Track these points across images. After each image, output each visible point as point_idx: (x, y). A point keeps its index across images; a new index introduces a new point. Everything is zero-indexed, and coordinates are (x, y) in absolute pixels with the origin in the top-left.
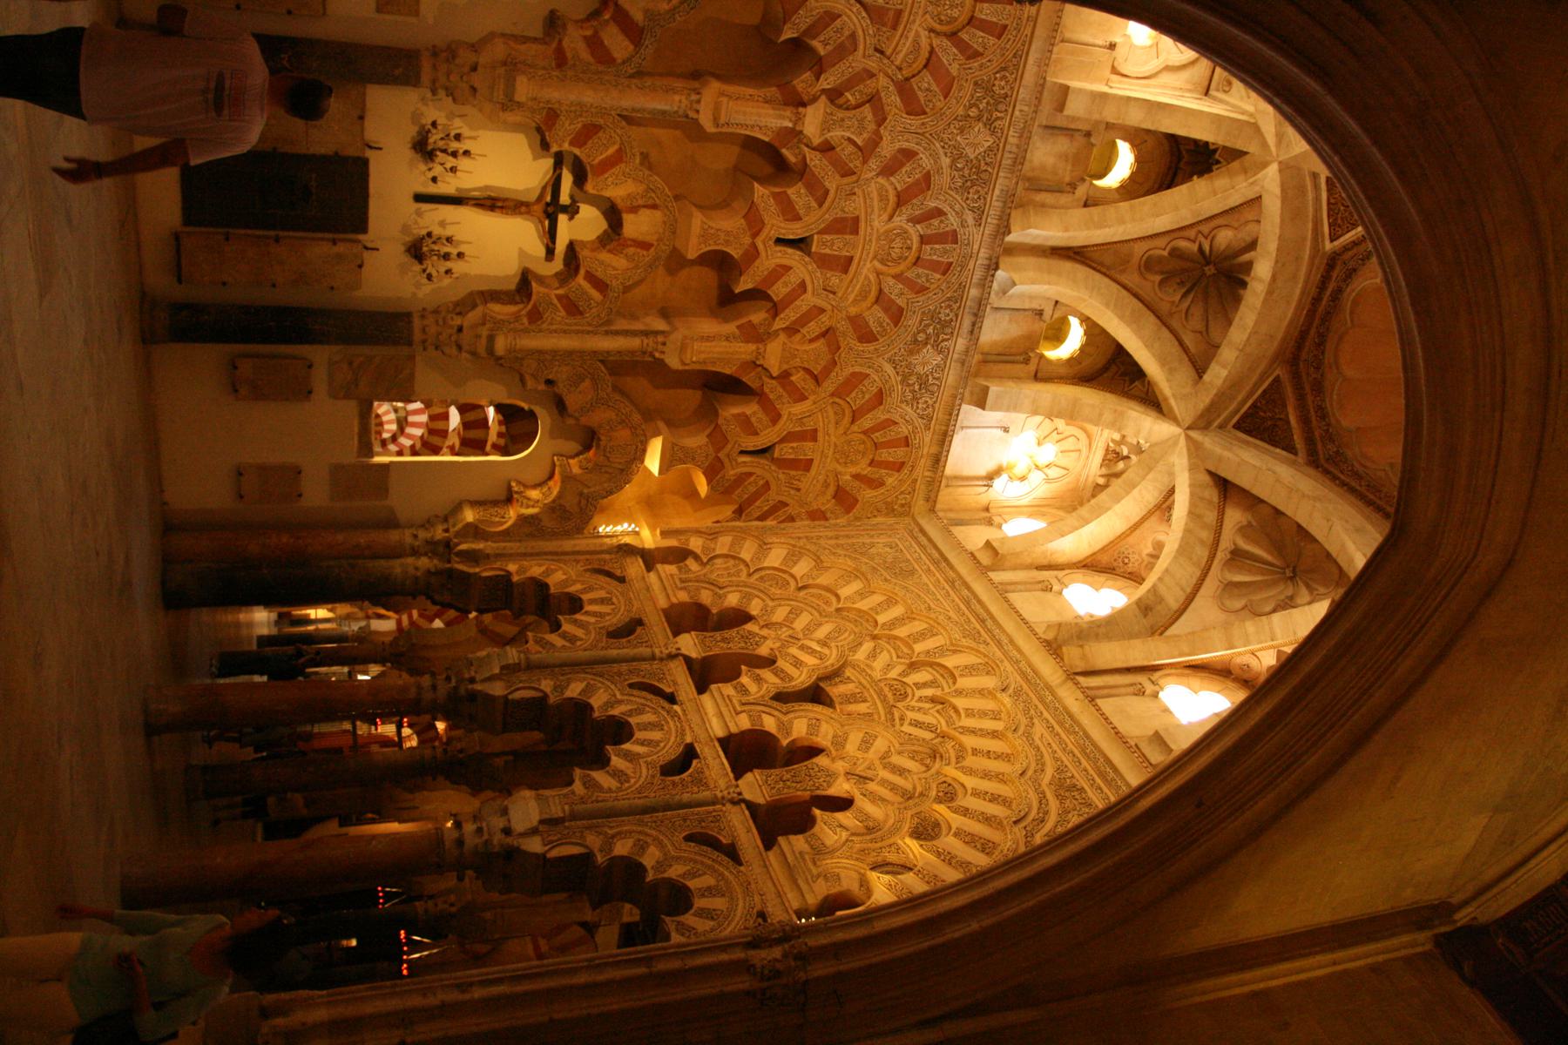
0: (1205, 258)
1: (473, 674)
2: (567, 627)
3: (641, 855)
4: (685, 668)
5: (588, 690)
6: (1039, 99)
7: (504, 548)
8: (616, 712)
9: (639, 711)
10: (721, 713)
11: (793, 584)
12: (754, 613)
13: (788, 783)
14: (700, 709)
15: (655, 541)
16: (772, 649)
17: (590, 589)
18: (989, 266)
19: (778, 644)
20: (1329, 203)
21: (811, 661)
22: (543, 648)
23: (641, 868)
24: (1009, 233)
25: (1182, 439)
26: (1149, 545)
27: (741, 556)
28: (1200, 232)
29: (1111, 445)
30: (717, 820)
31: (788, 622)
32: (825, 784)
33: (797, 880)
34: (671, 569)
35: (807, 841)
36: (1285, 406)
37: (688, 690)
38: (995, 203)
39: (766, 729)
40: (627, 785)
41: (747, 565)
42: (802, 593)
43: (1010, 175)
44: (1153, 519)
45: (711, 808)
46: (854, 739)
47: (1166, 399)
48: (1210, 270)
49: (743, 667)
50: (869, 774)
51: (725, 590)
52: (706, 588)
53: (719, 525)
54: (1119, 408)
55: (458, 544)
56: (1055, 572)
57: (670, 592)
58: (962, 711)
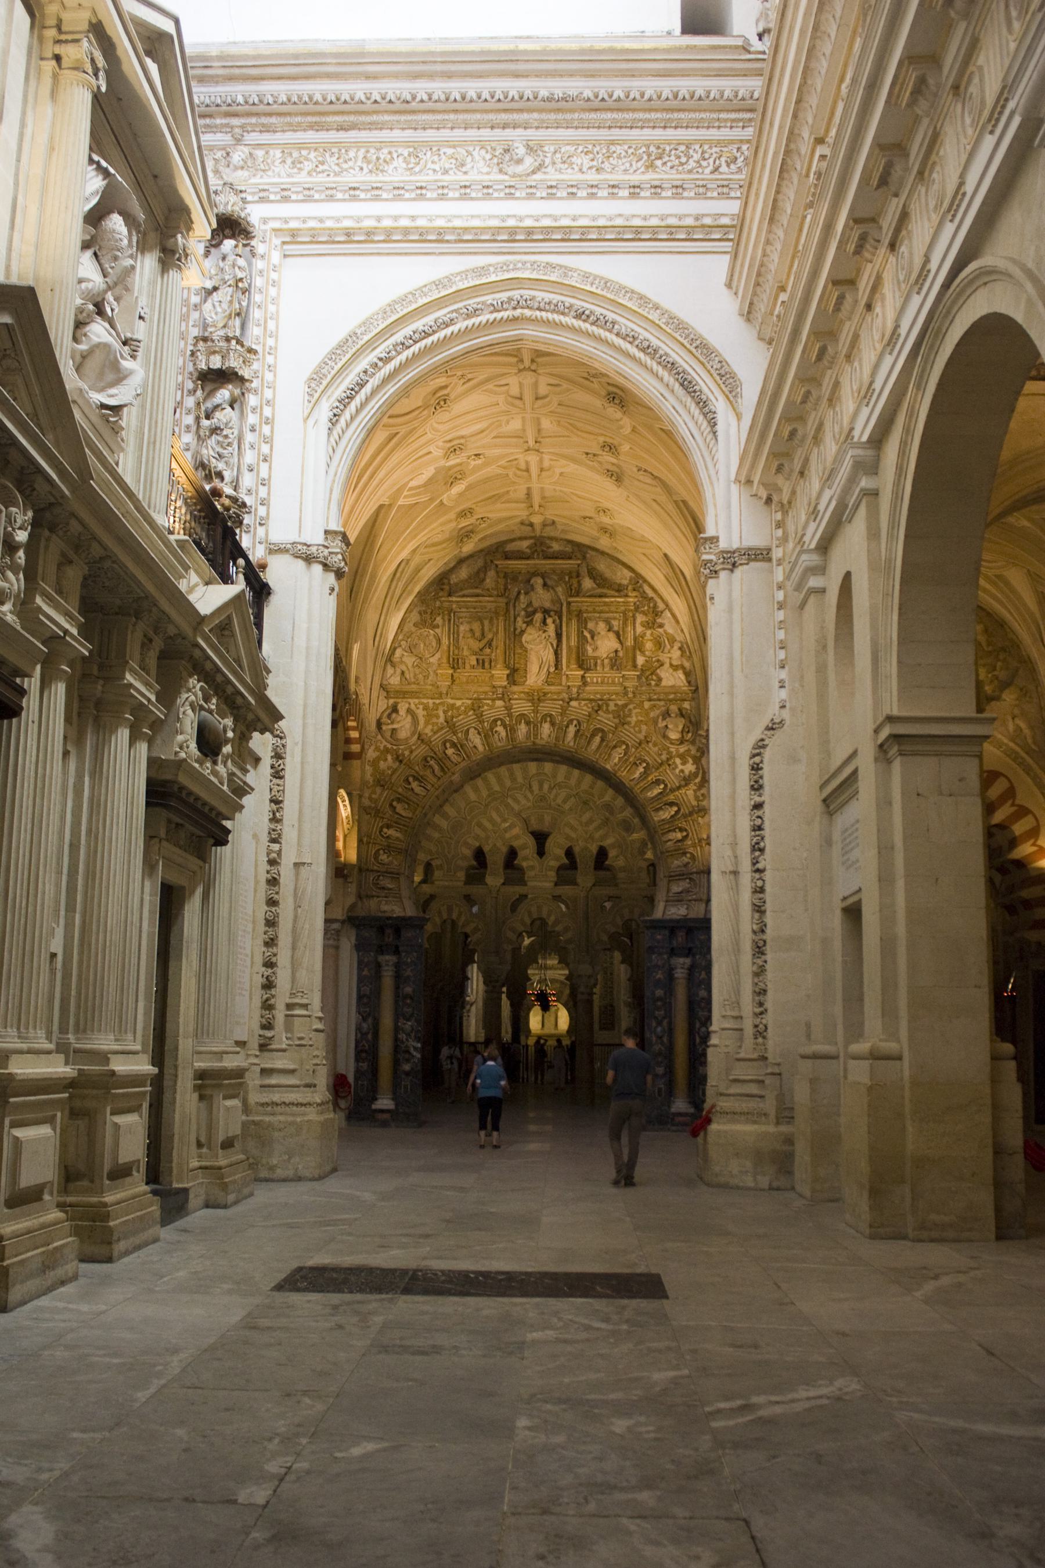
2: (468, 930)
8: (528, 921)
9: (530, 913)
12: (477, 844)
17: (440, 913)
21: (516, 831)
31: (485, 829)
34: (437, 874)
46: (567, 830)
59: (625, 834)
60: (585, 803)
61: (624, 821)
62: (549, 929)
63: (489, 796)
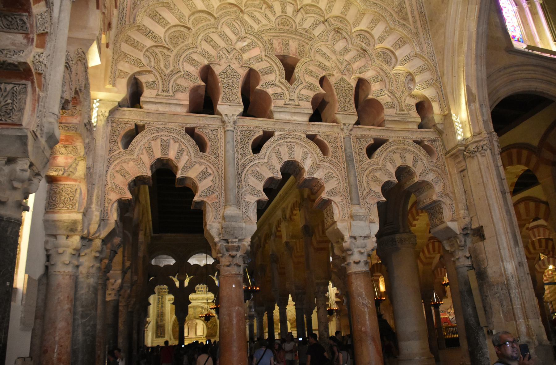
1: (237, 240)
3: (381, 181)
4: (248, 118)
5: (257, 175)
7: (98, 197)
8: (278, 167)
10: (294, 113)
11: (182, 29)
12: (206, 63)
13: (347, 101)
14: (283, 122)
15: (117, 93)
16: (241, 67)
17: (149, 149)
19: (235, 61)
21: (255, 52)
22: (213, 193)
23: (388, 183)
27: (148, 46)
30: (359, 139)
31: (215, 46)
32: (349, 86)
33: (408, 121)
34: (147, 95)
35: (389, 108)
37: (267, 122)
39: (312, 96)
40: (334, 175)
41: (156, 46)
42: (194, 30)
45: (352, 141)
49: (258, 87)
50: (345, 64)
51: (181, 69)
52: (176, 79)
53: (111, 46)
55: (89, 233)
57: (175, 102)
58: (313, 4)
59: (385, 66)
60: (337, 31)
61: (384, 53)
62: (306, 176)
63: (220, 8)
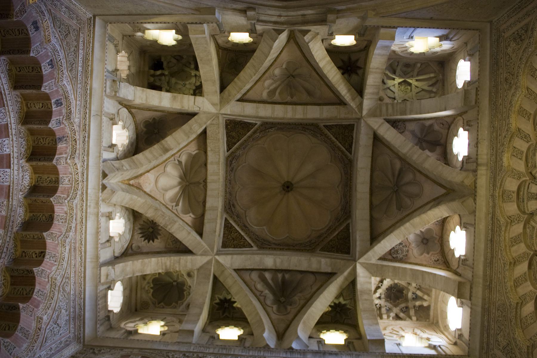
0: (277, 301)
6: (187, 343)
18: (290, 352)
20: (234, 248)
24: (267, 345)
25: (362, 260)
26: (423, 256)
28: (260, 295)
29: (391, 318)
36: (331, 240)
38: (251, 353)
43: (233, 350)
44: (409, 261)
47: (346, 279)
48: (282, 299)
54: (359, 293)
56: (458, 270)
58: (524, 158)
